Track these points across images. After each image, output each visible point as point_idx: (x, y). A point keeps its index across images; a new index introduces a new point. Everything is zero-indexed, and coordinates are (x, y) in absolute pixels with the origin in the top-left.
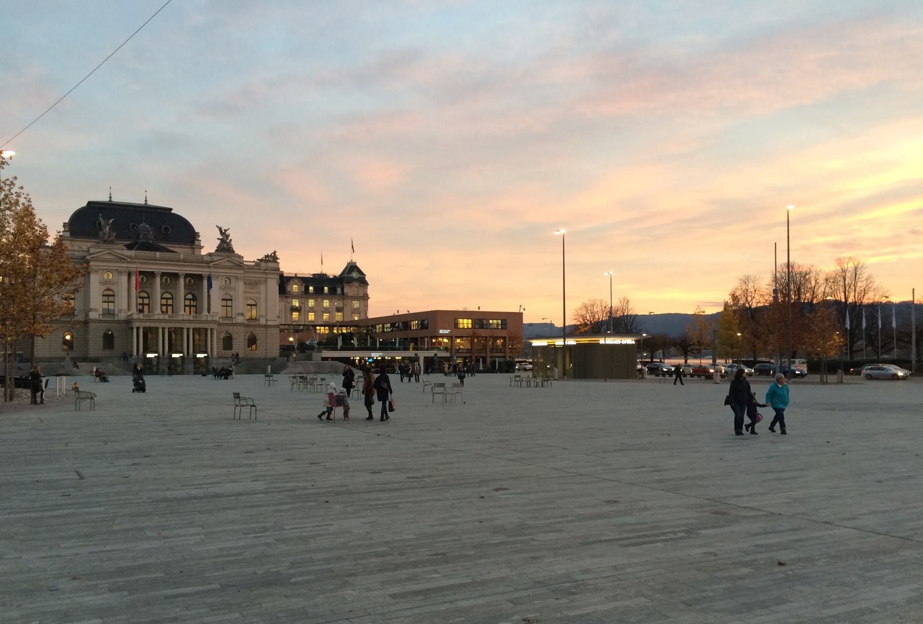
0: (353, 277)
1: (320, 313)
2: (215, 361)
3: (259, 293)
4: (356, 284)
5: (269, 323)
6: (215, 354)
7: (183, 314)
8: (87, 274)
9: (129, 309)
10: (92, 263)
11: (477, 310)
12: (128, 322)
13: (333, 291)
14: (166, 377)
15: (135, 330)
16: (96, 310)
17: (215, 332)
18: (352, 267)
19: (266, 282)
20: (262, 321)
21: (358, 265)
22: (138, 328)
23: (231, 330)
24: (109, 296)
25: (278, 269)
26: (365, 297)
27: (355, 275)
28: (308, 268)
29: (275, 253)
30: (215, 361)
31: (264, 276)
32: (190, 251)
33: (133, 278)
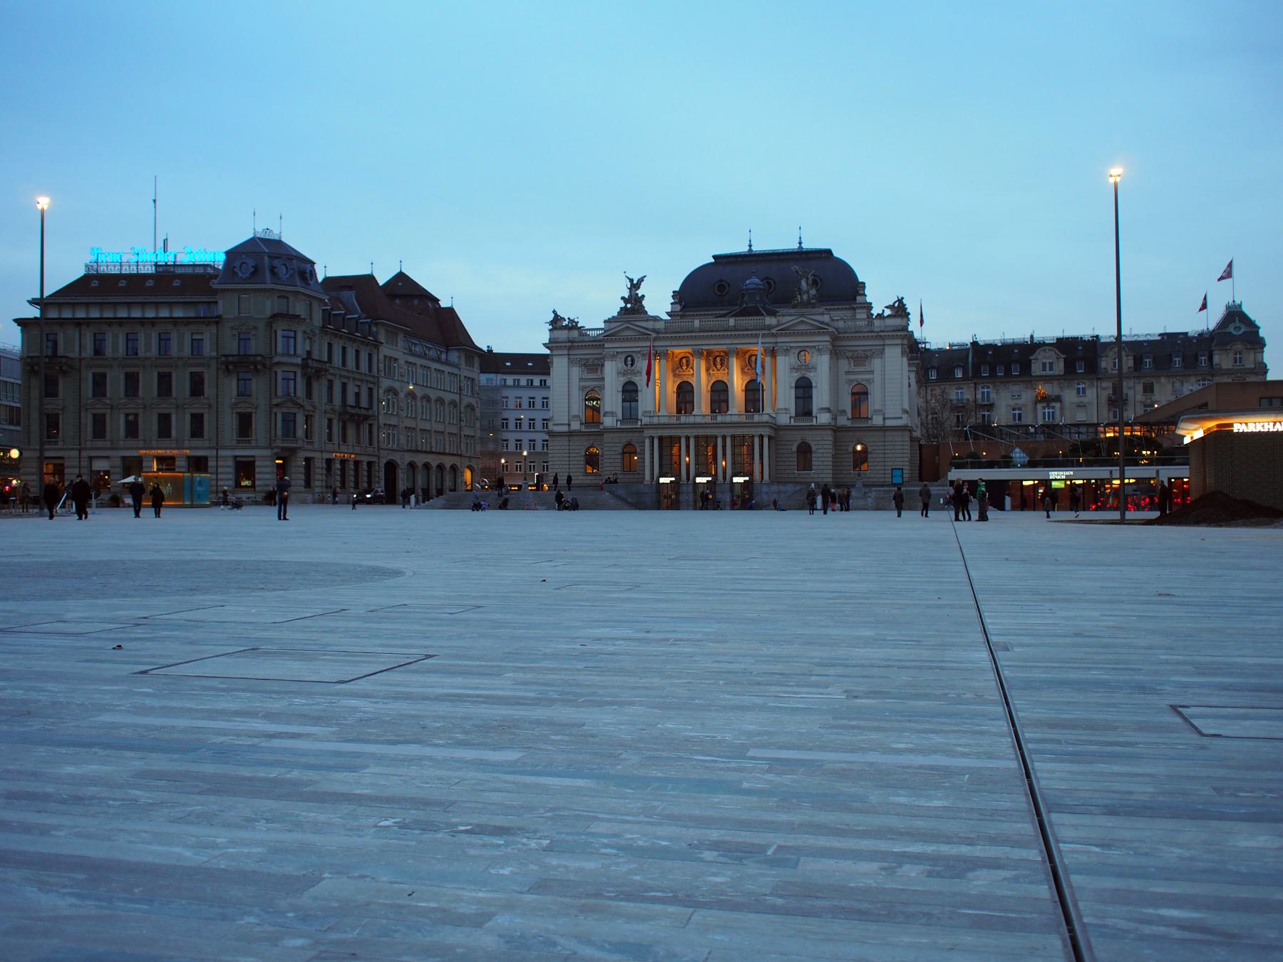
2: (765, 489)
3: (872, 372)
4: (1239, 347)
5: (889, 423)
14: (469, 514)
15: (647, 442)
16: (612, 414)
17: (766, 440)
18: (1235, 315)
19: (882, 352)
20: (877, 421)
21: (1246, 309)
23: (811, 438)
25: (905, 328)
26: (1263, 369)
30: (765, 489)
32: (849, 313)
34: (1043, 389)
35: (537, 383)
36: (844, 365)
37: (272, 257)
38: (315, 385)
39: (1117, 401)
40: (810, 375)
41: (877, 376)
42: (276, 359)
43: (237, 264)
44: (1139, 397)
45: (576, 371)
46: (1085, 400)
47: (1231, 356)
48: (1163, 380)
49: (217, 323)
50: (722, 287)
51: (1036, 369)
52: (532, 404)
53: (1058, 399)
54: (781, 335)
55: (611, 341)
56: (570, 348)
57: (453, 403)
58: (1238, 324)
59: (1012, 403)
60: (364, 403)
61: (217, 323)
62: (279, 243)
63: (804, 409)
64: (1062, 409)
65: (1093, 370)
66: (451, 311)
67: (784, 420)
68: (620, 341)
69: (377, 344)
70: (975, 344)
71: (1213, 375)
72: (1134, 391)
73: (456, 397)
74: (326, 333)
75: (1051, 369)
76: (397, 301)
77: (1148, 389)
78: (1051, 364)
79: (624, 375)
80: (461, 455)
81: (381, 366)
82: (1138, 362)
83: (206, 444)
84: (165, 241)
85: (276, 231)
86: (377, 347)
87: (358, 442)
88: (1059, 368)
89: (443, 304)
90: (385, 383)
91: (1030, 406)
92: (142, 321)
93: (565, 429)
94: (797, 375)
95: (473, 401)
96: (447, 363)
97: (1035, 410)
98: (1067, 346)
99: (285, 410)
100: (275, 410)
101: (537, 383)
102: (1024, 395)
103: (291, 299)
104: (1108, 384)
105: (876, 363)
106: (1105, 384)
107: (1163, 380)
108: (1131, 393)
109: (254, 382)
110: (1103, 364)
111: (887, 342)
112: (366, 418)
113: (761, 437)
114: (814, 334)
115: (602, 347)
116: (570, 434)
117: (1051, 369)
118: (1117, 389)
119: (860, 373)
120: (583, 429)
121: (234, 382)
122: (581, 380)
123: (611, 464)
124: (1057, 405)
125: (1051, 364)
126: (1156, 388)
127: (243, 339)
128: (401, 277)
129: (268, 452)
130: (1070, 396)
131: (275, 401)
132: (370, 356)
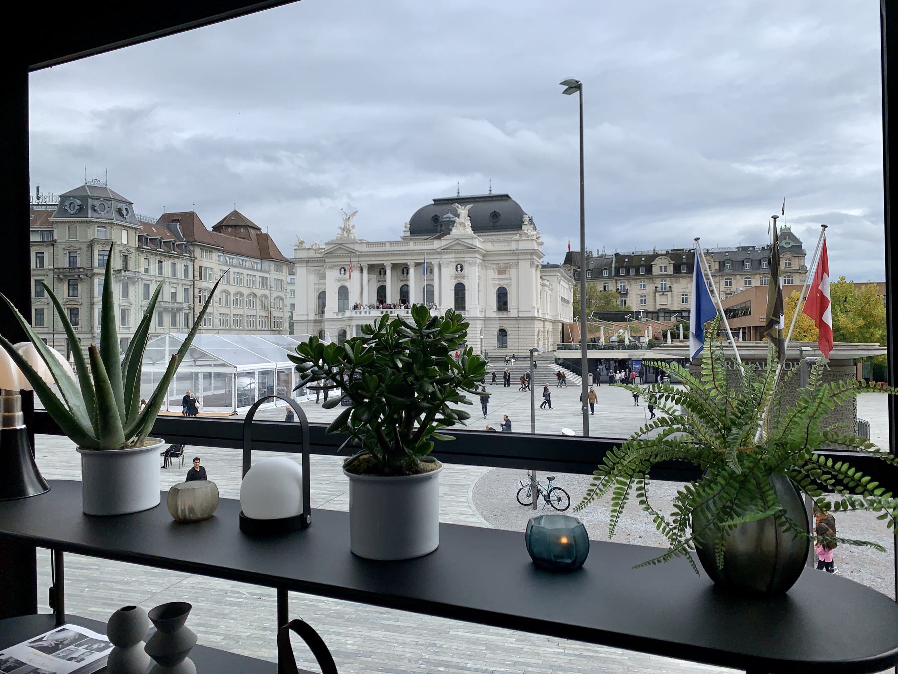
3: (510, 278)
34: (658, 283)
38: (132, 290)
40: (462, 281)
43: (67, 203)
45: (313, 278)
48: (738, 277)
49: (53, 245)
50: (436, 219)
51: (656, 270)
55: (330, 257)
56: (308, 262)
57: (265, 296)
60: (180, 297)
61: (53, 245)
64: (672, 296)
66: (267, 235)
68: (335, 257)
69: (193, 259)
70: (617, 254)
73: (267, 292)
74: (142, 252)
75: (665, 270)
76: (230, 229)
78: (665, 267)
79: (339, 281)
81: (197, 274)
82: (722, 264)
83: (46, 330)
84: (38, 188)
87: (174, 323)
88: (671, 269)
89: (264, 231)
91: (652, 294)
93: (305, 318)
95: (282, 294)
97: (655, 296)
107: (738, 277)
109: (80, 286)
111: (520, 257)
112: (179, 309)
114: (464, 252)
116: (308, 321)
117: (665, 270)
121: (66, 286)
122: (315, 284)
124: (669, 294)
125: (665, 267)
127: (72, 258)
128: (236, 213)
132: (186, 266)
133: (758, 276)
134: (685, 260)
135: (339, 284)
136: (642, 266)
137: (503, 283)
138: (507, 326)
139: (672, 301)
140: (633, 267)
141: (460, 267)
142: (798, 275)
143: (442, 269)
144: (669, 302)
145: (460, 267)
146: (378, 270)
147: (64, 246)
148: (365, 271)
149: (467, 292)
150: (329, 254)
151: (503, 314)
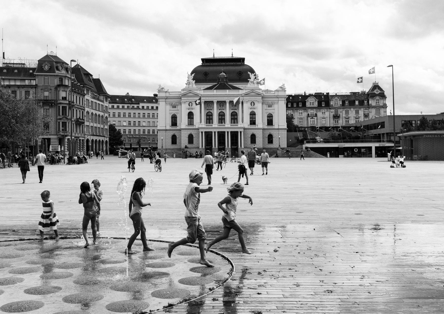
0: (377, 93)
1: (353, 117)
4: (378, 98)
5: (280, 127)
6: (243, 147)
7: (228, 123)
8: (181, 104)
9: (201, 122)
10: (182, 98)
11: (420, 114)
12: (198, 129)
13: (361, 103)
15: (200, 134)
17: (242, 133)
18: (376, 86)
20: (276, 126)
21: (379, 85)
22: (202, 132)
23: (255, 132)
24: (191, 115)
27: (377, 92)
28: (345, 91)
29: (284, 85)
31: (277, 99)
33: (203, 105)
34: (310, 112)
35: (121, 107)
36: (265, 107)
37: (57, 63)
39: (336, 117)
40: (255, 110)
41: (276, 111)
42: (59, 102)
44: (344, 115)
45: (169, 107)
46: (325, 116)
47: (375, 101)
48: (352, 109)
49: (35, 87)
51: (308, 105)
52: (119, 116)
53: (316, 115)
54: (245, 96)
56: (166, 99)
58: (377, 90)
59: (299, 117)
60: (81, 118)
61: (35, 87)
62: (56, 57)
63: (253, 122)
64: (317, 119)
65: (328, 105)
67: (246, 126)
71: (369, 108)
72: (342, 113)
75: (313, 105)
77: (347, 113)
80: (104, 136)
82: (344, 102)
85: (55, 52)
86: (84, 96)
88: (316, 104)
89: (94, 77)
90: (87, 109)
91: (306, 118)
92: (19, 87)
93: (164, 128)
94: (251, 110)
96: (98, 99)
97: (308, 119)
98: (318, 96)
99: (63, 121)
100: (58, 121)
101: (121, 107)
102: (303, 114)
103: (64, 79)
104: (333, 110)
105: (275, 106)
106: (332, 111)
107: (352, 109)
108: (341, 114)
109: (50, 109)
110: (331, 103)
111: (279, 99)
113: (241, 132)
114: (257, 96)
115: (181, 98)
116: (166, 130)
117: (313, 105)
118: (336, 112)
119: (270, 110)
120: (171, 128)
123: (184, 141)
124: (316, 118)
125: (313, 103)
126: (350, 112)
129: (56, 137)
130: (320, 114)
131: (59, 117)
133: (362, 109)
134: (323, 99)
135: (189, 111)
136: (300, 102)
137: (271, 112)
138: (273, 132)
139: (317, 122)
140: (295, 102)
141: (253, 103)
142: (383, 109)
143: (244, 105)
144: (316, 123)
145: (253, 103)
146: (209, 104)
147: (41, 88)
148: (203, 105)
149: (194, 116)
150: (184, 95)
151: (270, 127)
